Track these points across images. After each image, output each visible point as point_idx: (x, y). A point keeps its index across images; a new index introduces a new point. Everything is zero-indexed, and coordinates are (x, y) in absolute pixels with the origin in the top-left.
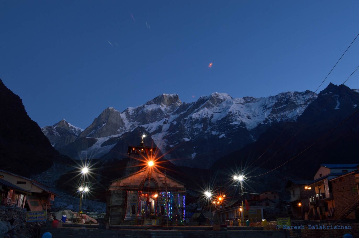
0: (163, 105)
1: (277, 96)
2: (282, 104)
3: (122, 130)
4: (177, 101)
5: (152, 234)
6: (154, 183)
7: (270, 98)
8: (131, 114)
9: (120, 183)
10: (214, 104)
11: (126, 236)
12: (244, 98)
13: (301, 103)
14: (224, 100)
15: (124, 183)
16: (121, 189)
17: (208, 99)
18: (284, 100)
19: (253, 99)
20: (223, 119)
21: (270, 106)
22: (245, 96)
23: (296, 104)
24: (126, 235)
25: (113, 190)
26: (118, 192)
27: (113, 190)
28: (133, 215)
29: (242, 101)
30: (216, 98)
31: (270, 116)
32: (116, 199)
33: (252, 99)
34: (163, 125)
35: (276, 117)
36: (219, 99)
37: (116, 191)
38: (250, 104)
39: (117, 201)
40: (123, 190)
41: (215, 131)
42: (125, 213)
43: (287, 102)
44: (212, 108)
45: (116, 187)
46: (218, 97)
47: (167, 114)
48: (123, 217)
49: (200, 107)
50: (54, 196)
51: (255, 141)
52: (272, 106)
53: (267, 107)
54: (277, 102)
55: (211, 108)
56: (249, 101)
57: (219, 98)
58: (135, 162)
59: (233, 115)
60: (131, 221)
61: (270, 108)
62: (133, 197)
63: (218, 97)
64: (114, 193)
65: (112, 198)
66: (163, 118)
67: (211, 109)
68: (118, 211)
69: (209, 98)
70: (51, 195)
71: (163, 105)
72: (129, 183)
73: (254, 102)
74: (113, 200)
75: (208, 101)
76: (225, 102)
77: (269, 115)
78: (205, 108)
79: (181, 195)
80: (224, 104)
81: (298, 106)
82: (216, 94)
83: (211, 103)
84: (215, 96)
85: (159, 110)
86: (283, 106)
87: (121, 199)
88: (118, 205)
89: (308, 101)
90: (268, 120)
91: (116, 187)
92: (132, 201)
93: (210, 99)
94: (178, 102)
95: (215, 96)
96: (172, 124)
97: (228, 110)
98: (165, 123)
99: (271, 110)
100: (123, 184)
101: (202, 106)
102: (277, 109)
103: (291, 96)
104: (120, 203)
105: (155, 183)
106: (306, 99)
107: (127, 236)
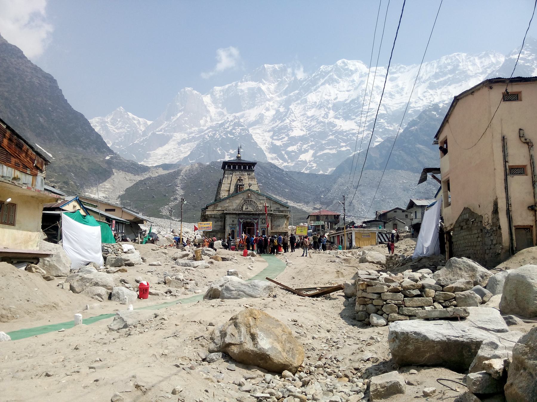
0: (264, 82)
2: (445, 74)
3: (206, 121)
4: (284, 76)
8: (218, 98)
10: (341, 78)
13: (478, 71)
14: (356, 70)
18: (449, 67)
20: (353, 101)
21: (427, 78)
23: (469, 72)
30: (343, 69)
31: (425, 94)
36: (347, 69)
41: (341, 119)
43: (452, 71)
44: (337, 85)
46: (346, 67)
47: (271, 95)
49: (320, 83)
54: (438, 71)
57: (348, 68)
61: (427, 80)
63: (346, 67)
66: (265, 102)
69: (332, 69)
71: (264, 82)
73: (401, 73)
75: (331, 74)
77: (425, 92)
78: (327, 85)
80: (356, 77)
81: (472, 76)
82: (344, 62)
83: (336, 77)
84: (342, 65)
85: (259, 89)
86: (447, 77)
89: (489, 68)
90: (422, 100)
93: (334, 69)
94: (287, 78)
95: (342, 65)
96: (278, 111)
98: (268, 110)
99: (428, 83)
101: (322, 81)
102: (438, 82)
103: (461, 61)
106: (485, 64)
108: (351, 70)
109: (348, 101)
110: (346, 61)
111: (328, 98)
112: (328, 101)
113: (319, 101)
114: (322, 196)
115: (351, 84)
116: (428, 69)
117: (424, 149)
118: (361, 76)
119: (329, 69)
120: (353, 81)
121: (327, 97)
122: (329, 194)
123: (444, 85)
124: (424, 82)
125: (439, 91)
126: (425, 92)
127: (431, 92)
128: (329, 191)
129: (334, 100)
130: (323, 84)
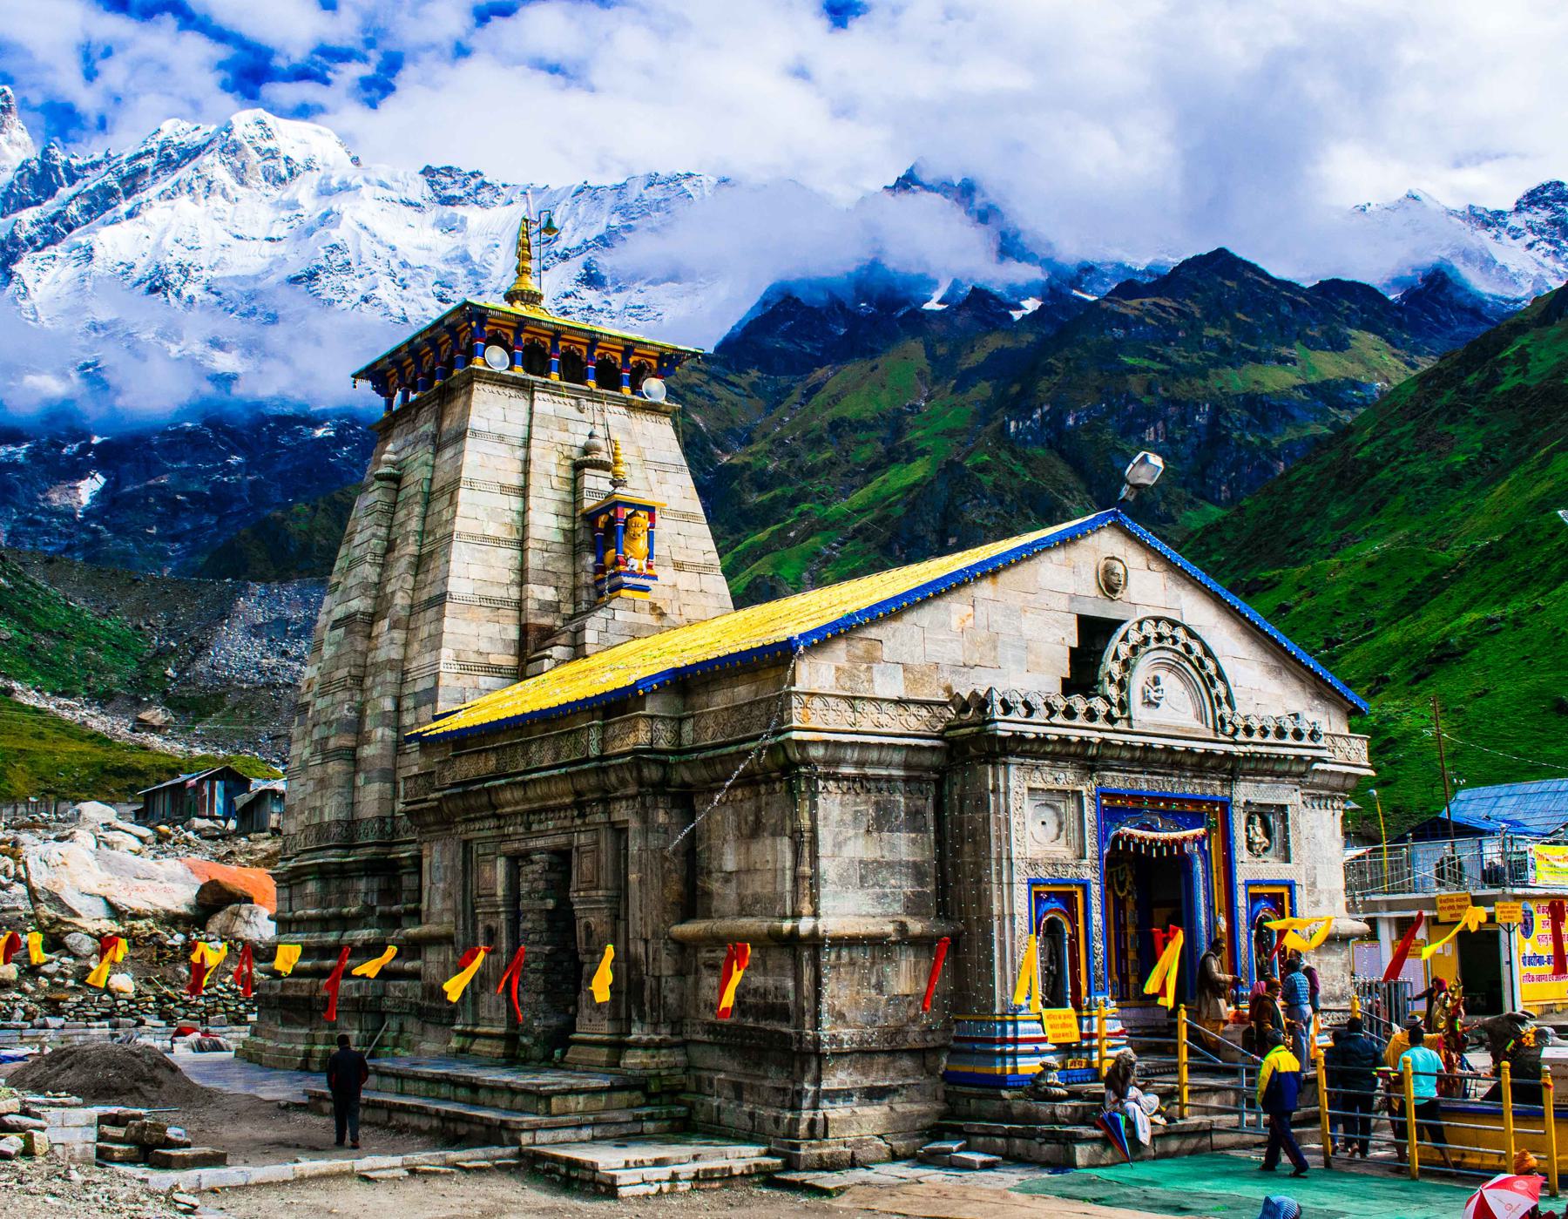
1: (620, 189)
7: (580, 191)
12: (428, 171)
17: (205, 146)
19: (484, 184)
21: (575, 242)
22: (436, 165)
29: (419, 189)
30: (258, 150)
31: (566, 302)
33: (473, 182)
35: (601, 311)
36: (273, 154)
38: (459, 210)
46: (270, 144)
52: (585, 242)
55: (220, 206)
56: (458, 192)
59: (353, 265)
67: (218, 215)
69: (211, 142)
73: (483, 205)
76: (313, 178)
80: (303, 190)
93: (217, 146)
95: (256, 131)
97: (323, 231)
99: (575, 266)
101: (167, 182)
108: (288, 160)
111: (188, 258)
112: (184, 270)
113: (145, 261)
114: (170, 672)
115: (285, 214)
116: (581, 210)
118: (325, 191)
119: (199, 138)
120: (293, 205)
121: (181, 255)
122: (200, 666)
124: (565, 258)
125: (617, 301)
126: (567, 296)
127: (591, 296)
128: (200, 650)
129: (212, 268)
130: (168, 196)
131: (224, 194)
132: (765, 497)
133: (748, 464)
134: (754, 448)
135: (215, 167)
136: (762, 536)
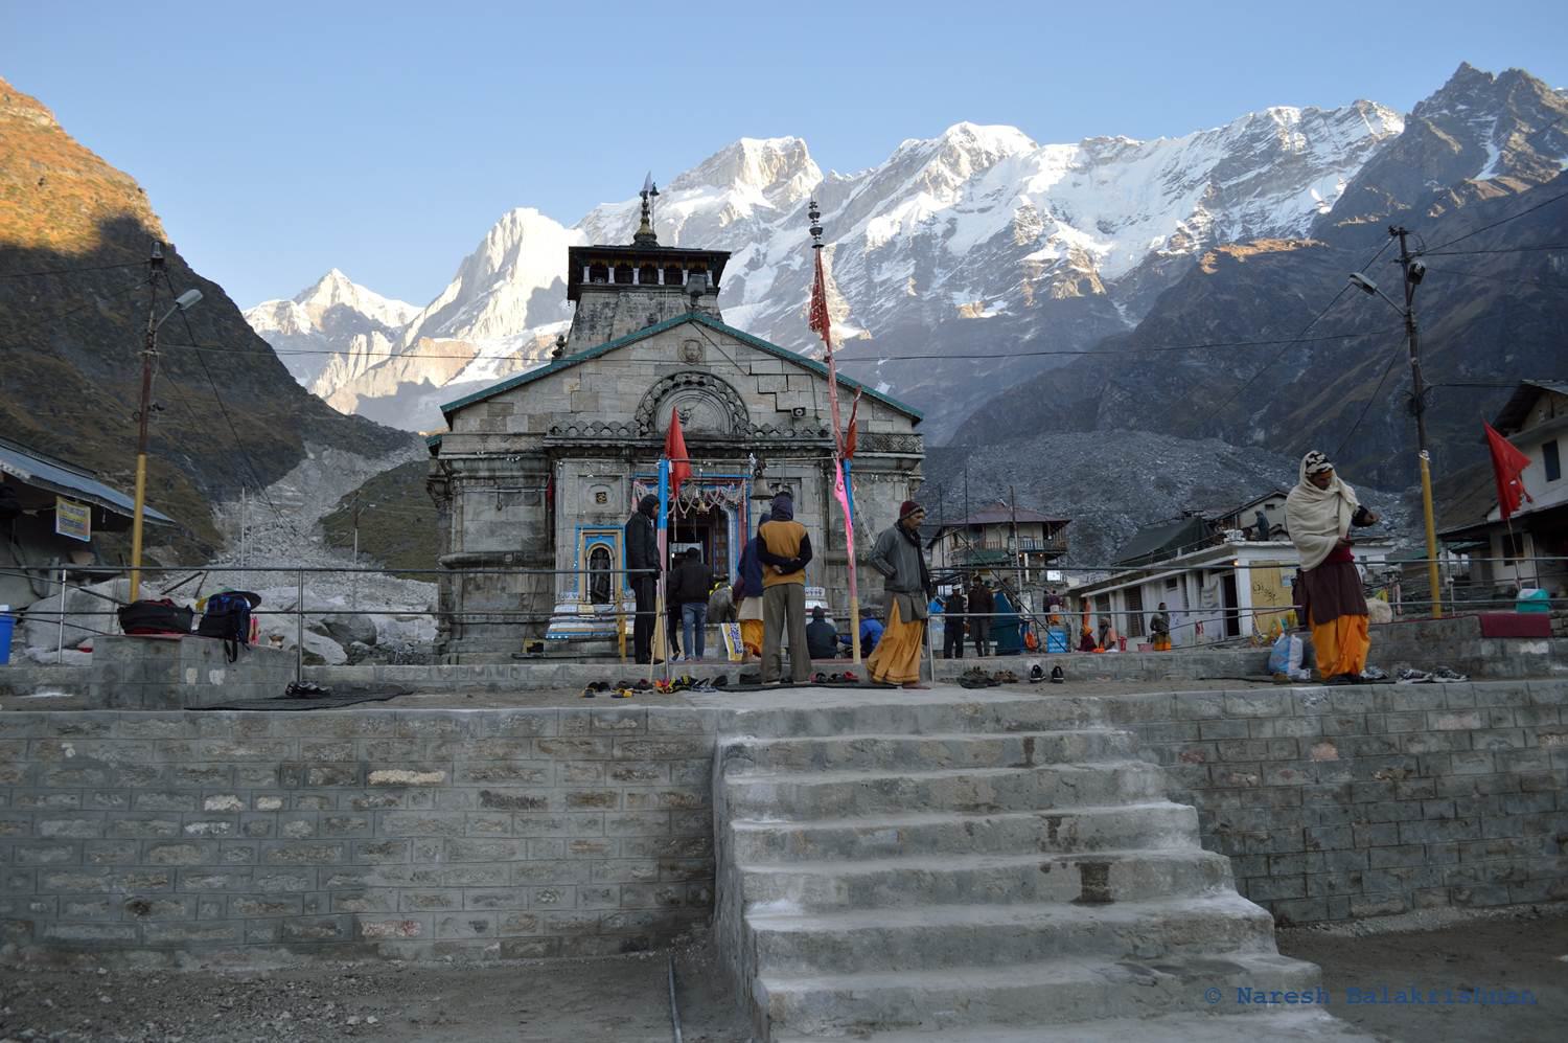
5: (738, 750)
6: (725, 404)
9: (505, 417)
11: (384, 786)
15: (530, 417)
16: (516, 452)
18: (1261, 147)
24: (377, 776)
25: (465, 460)
26: (498, 474)
27: (464, 456)
28: (602, 608)
32: (490, 515)
33: (1120, 146)
34: (747, 274)
35: (1222, 222)
37: (481, 464)
39: (493, 530)
40: (534, 455)
41: (966, 290)
42: (549, 597)
45: (484, 436)
48: (539, 625)
49: (899, 192)
50: (88, 509)
51: (1133, 325)
53: (1185, 180)
56: (1105, 154)
58: (607, 330)
60: (588, 645)
62: (593, 499)
64: (470, 478)
65: (462, 507)
68: (503, 589)
69: (935, 150)
70: (60, 501)
72: (564, 414)
74: (466, 523)
79: (896, 478)
81: (1319, 171)
82: (965, 132)
87: (523, 513)
88: (504, 549)
90: (1189, 236)
91: (484, 436)
92: (588, 522)
95: (962, 137)
96: (783, 270)
100: (526, 422)
101: (909, 184)
102: (1229, 188)
104: (513, 541)
105: (732, 408)
106: (1352, 139)
107: (402, 787)
109: (984, 239)
110: (971, 127)
117: (1206, 370)
123: (1247, 193)
124: (1191, 187)
131: (947, 184)
132: (1355, 343)
133: (1340, 320)
134: (1345, 306)
135: (937, 166)
136: (1356, 371)
